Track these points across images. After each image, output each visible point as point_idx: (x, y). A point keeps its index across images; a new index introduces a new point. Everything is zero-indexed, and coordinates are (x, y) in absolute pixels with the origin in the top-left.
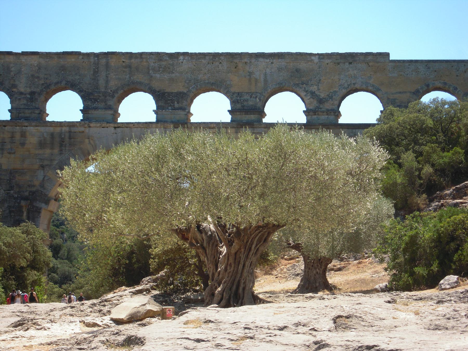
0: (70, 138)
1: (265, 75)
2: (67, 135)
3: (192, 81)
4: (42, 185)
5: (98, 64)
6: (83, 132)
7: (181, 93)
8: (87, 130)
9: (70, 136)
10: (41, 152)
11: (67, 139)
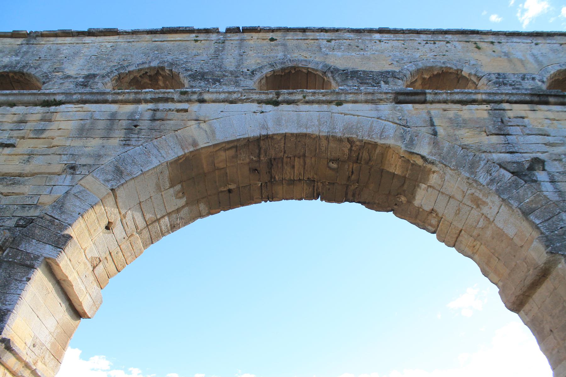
0: (153, 120)
1: (533, 55)
2: (148, 115)
3: (405, 59)
4: (60, 205)
5: (224, 42)
6: (186, 111)
7: (388, 72)
8: (194, 108)
9: (154, 115)
10: (78, 143)
11: (145, 124)
